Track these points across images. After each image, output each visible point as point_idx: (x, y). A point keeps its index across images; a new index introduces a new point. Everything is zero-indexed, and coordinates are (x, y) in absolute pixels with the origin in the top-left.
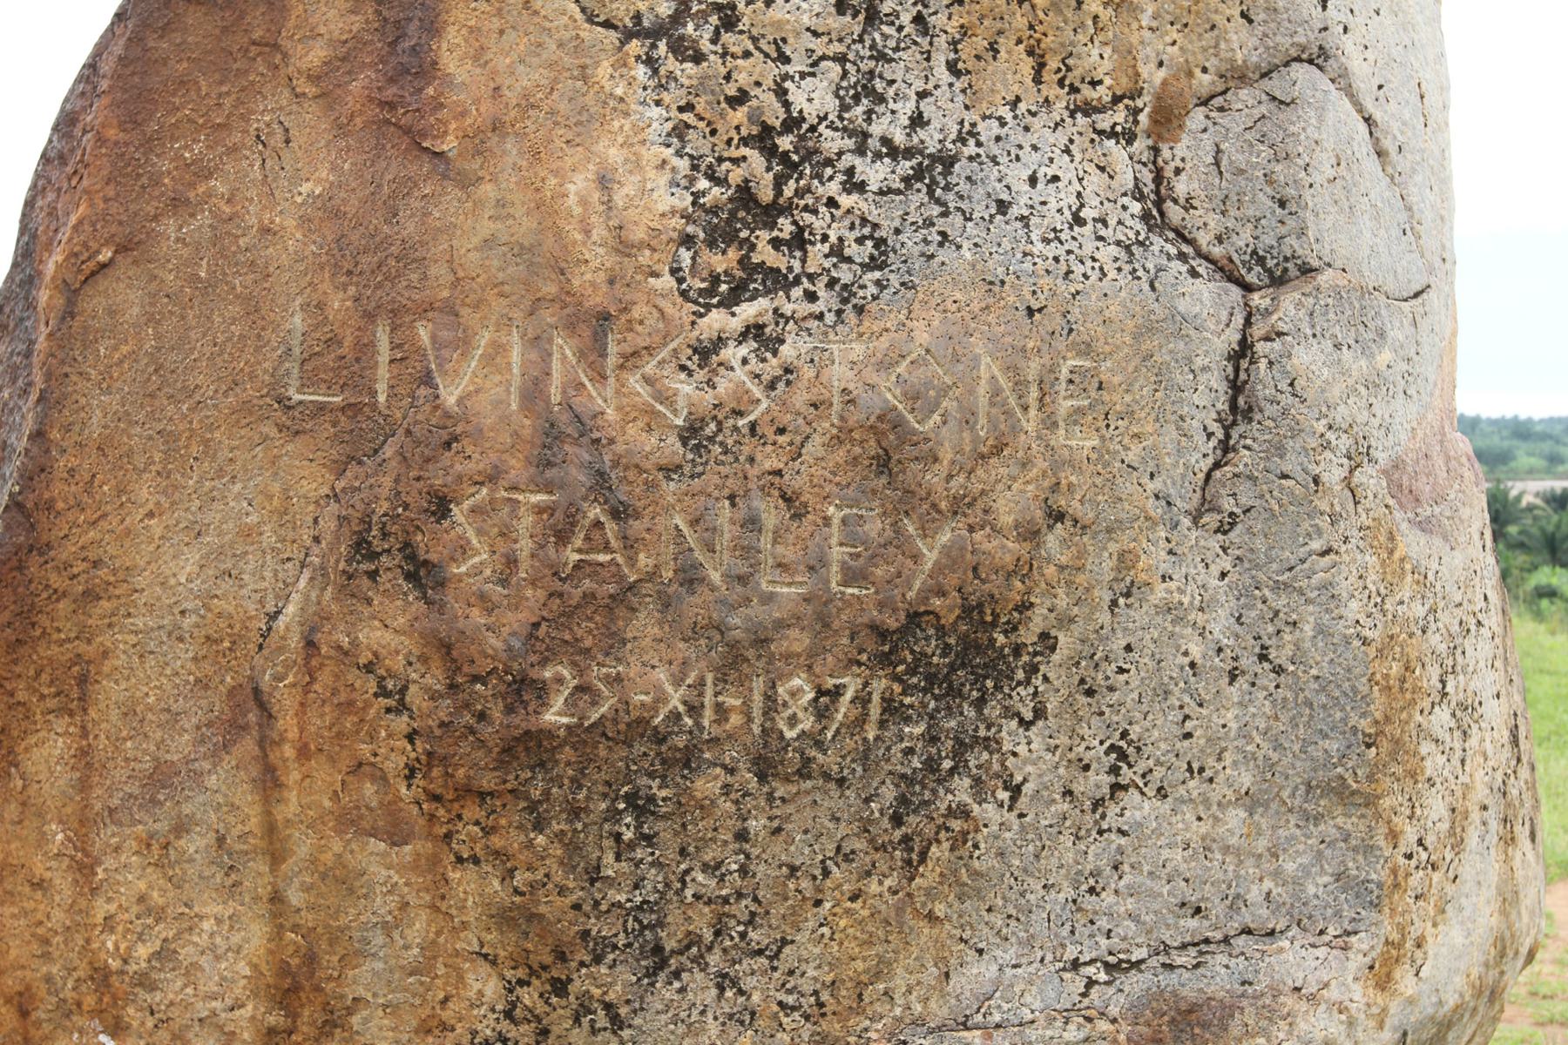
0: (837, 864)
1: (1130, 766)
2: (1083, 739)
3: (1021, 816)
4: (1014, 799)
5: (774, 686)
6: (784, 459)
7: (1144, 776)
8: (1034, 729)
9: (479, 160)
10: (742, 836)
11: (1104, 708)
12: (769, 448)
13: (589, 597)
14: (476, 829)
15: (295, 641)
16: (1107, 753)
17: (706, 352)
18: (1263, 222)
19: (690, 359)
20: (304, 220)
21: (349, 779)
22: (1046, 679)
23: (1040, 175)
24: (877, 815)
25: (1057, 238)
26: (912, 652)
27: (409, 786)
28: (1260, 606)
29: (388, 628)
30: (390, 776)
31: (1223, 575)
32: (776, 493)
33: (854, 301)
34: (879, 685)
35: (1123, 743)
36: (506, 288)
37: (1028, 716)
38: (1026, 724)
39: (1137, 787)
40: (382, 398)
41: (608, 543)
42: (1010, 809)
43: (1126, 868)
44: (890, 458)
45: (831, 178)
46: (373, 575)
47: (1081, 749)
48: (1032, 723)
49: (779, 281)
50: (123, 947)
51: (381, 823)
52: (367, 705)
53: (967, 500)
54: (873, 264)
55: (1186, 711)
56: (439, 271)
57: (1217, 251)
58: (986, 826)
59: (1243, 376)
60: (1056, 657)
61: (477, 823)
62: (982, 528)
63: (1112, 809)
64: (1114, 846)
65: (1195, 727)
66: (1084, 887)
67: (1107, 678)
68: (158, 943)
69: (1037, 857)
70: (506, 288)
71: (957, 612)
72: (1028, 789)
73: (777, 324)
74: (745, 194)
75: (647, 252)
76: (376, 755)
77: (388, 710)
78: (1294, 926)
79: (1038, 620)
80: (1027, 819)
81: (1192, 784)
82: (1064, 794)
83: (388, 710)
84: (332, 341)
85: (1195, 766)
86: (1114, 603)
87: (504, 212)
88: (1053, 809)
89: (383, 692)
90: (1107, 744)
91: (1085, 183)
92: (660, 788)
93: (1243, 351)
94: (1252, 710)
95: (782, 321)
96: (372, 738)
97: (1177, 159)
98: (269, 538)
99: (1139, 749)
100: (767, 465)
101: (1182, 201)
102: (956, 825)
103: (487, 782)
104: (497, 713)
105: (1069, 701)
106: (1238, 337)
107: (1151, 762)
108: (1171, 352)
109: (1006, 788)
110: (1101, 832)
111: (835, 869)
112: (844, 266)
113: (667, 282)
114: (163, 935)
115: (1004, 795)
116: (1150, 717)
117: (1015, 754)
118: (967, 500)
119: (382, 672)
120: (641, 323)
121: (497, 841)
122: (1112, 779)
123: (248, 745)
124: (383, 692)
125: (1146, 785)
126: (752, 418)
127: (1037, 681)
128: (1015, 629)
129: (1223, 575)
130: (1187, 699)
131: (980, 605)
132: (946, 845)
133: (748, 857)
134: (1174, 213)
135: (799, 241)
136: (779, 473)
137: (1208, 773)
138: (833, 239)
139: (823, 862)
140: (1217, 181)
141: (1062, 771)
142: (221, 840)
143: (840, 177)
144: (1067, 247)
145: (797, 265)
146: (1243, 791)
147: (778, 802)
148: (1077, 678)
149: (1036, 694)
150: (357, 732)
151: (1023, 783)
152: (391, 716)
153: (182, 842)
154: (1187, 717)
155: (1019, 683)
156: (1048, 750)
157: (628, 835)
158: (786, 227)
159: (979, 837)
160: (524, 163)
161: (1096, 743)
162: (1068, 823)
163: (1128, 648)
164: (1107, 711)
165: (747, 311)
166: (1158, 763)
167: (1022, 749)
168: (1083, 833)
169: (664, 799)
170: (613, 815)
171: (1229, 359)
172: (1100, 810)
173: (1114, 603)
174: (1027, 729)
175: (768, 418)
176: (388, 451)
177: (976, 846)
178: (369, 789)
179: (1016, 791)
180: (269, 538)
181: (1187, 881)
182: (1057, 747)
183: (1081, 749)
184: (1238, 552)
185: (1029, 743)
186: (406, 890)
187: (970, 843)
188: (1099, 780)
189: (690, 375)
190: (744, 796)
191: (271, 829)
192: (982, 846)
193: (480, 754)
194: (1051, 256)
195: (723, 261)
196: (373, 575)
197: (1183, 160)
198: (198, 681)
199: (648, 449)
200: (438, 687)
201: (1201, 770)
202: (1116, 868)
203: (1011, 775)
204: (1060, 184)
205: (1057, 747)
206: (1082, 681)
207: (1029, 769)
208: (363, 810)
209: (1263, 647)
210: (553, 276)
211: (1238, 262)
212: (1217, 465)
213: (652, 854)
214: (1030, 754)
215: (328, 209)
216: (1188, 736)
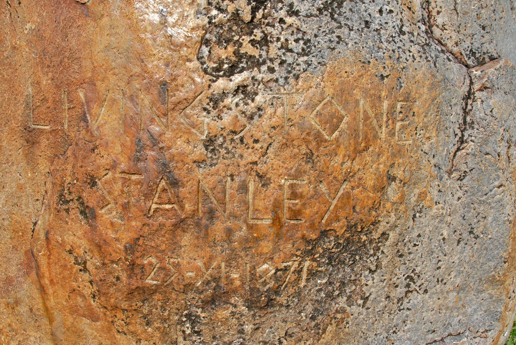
0: (285, 339)
1: (414, 283)
2: (396, 275)
3: (368, 308)
4: (364, 303)
5: (255, 268)
6: (258, 156)
7: (419, 286)
8: (376, 273)
9: (102, 6)
10: (241, 332)
11: (406, 262)
12: (250, 150)
13: (162, 226)
14: (123, 322)
15: (42, 236)
16: (406, 279)
17: (216, 101)
18: (475, 36)
19: (208, 104)
20: (29, 42)
21: (71, 295)
22: (383, 252)
23: (384, 10)
24: (304, 318)
25: (393, 40)
26: (323, 248)
27: (94, 301)
28: (472, 211)
29: (75, 234)
30: (86, 296)
31: (459, 198)
32: (254, 173)
33: (294, 72)
34: (307, 264)
35: (412, 275)
36: (116, 71)
37: (373, 268)
38: (371, 272)
39: (416, 290)
40: (66, 126)
41: (169, 199)
42: (363, 306)
43: (409, 322)
44: (313, 154)
45: (281, 9)
46: (67, 211)
47: (395, 279)
48: (375, 271)
49: (255, 63)
50: (7, 340)
51: (87, 313)
52: (72, 268)
53: (351, 174)
54: (304, 53)
55: (439, 258)
56: (87, 63)
57: (455, 50)
58: (352, 315)
59: (469, 107)
60: (388, 243)
61: (123, 320)
62: (358, 187)
63: (406, 300)
64: (404, 315)
65: (442, 265)
66: (391, 331)
67: (409, 249)
68: (17, 342)
69: (373, 324)
70: (116, 71)
71: (345, 228)
72: (372, 297)
73: (254, 85)
74: (236, 16)
75: (185, 49)
76: (79, 287)
77: (81, 270)
78: (467, 330)
79: (382, 228)
80: (370, 310)
81: (438, 286)
82: (386, 298)
83: (81, 270)
84: (45, 100)
85: (440, 279)
86: (414, 216)
87: (114, 31)
88: (381, 304)
89: (77, 263)
90: (406, 276)
91: (403, 14)
92: (202, 312)
93: (469, 96)
94: (465, 254)
95: (256, 83)
96: (76, 280)
97: (438, 7)
98: (29, 190)
99: (419, 276)
100: (250, 159)
101: (440, 26)
102: (339, 316)
103: (124, 305)
104: (124, 277)
105: (392, 261)
106: (468, 89)
107: (423, 281)
108: (443, 97)
109: (362, 299)
110: (400, 310)
111: (285, 341)
112: (289, 54)
113: (195, 64)
114: (19, 339)
115: (360, 302)
116: (425, 263)
117: (367, 285)
118: (351, 174)
119: (75, 254)
120: (183, 86)
121: (131, 327)
122: (407, 289)
123: (34, 274)
124: (77, 263)
125: (420, 289)
126: (241, 134)
127: (379, 254)
128: (371, 232)
129: (459, 198)
130: (441, 254)
131: (356, 225)
132: (334, 325)
133: (244, 339)
134: (437, 32)
135: (265, 41)
136: (255, 163)
137: (445, 281)
138: (282, 40)
139: (279, 339)
140: (456, 17)
141: (386, 289)
142: (31, 310)
143: (286, 8)
144: (398, 45)
145: (264, 53)
146: (456, 285)
147: (258, 318)
148: (396, 250)
149: (378, 259)
150: (70, 277)
151: (369, 296)
152: (82, 273)
153: (18, 308)
154: (440, 261)
155: (371, 255)
156: (381, 281)
157: (188, 332)
158: (258, 34)
159: (349, 319)
160: (123, 5)
161: (402, 276)
162: (387, 309)
163: (419, 236)
164: (407, 262)
165: (238, 78)
166: (426, 281)
167: (370, 283)
168: (393, 312)
169: (203, 317)
170: (181, 323)
171: (463, 99)
172: (401, 302)
173: (414, 216)
174: (373, 274)
175: (249, 134)
176: (69, 153)
177: (347, 323)
178: (80, 299)
179: (366, 299)
180: (29, 190)
181: (431, 323)
182: (385, 279)
183: (395, 279)
184: (466, 189)
185: (373, 280)
186: (100, 338)
187: (345, 322)
188: (401, 291)
189: (209, 113)
190: (241, 316)
191: (47, 309)
192: (350, 323)
193: (119, 294)
194: (391, 49)
195: (225, 53)
196: (67, 211)
197: (441, 7)
198: (13, 247)
199: (188, 152)
200: (98, 264)
201: (442, 280)
202: (404, 322)
203: (365, 294)
204: (394, 14)
205: (385, 279)
206: (398, 251)
207: (373, 290)
208: (79, 307)
209: (472, 228)
210: (139, 63)
211: (464, 55)
212: (458, 149)
213: (200, 339)
214: (373, 285)
215: (38, 35)
216: (439, 268)
